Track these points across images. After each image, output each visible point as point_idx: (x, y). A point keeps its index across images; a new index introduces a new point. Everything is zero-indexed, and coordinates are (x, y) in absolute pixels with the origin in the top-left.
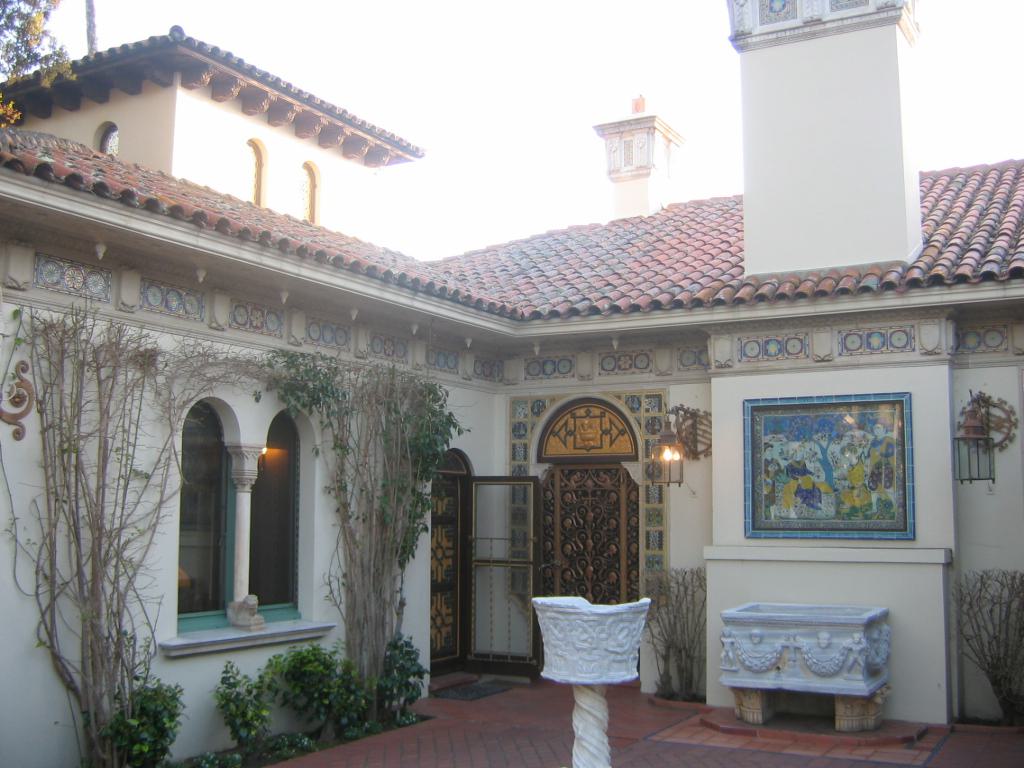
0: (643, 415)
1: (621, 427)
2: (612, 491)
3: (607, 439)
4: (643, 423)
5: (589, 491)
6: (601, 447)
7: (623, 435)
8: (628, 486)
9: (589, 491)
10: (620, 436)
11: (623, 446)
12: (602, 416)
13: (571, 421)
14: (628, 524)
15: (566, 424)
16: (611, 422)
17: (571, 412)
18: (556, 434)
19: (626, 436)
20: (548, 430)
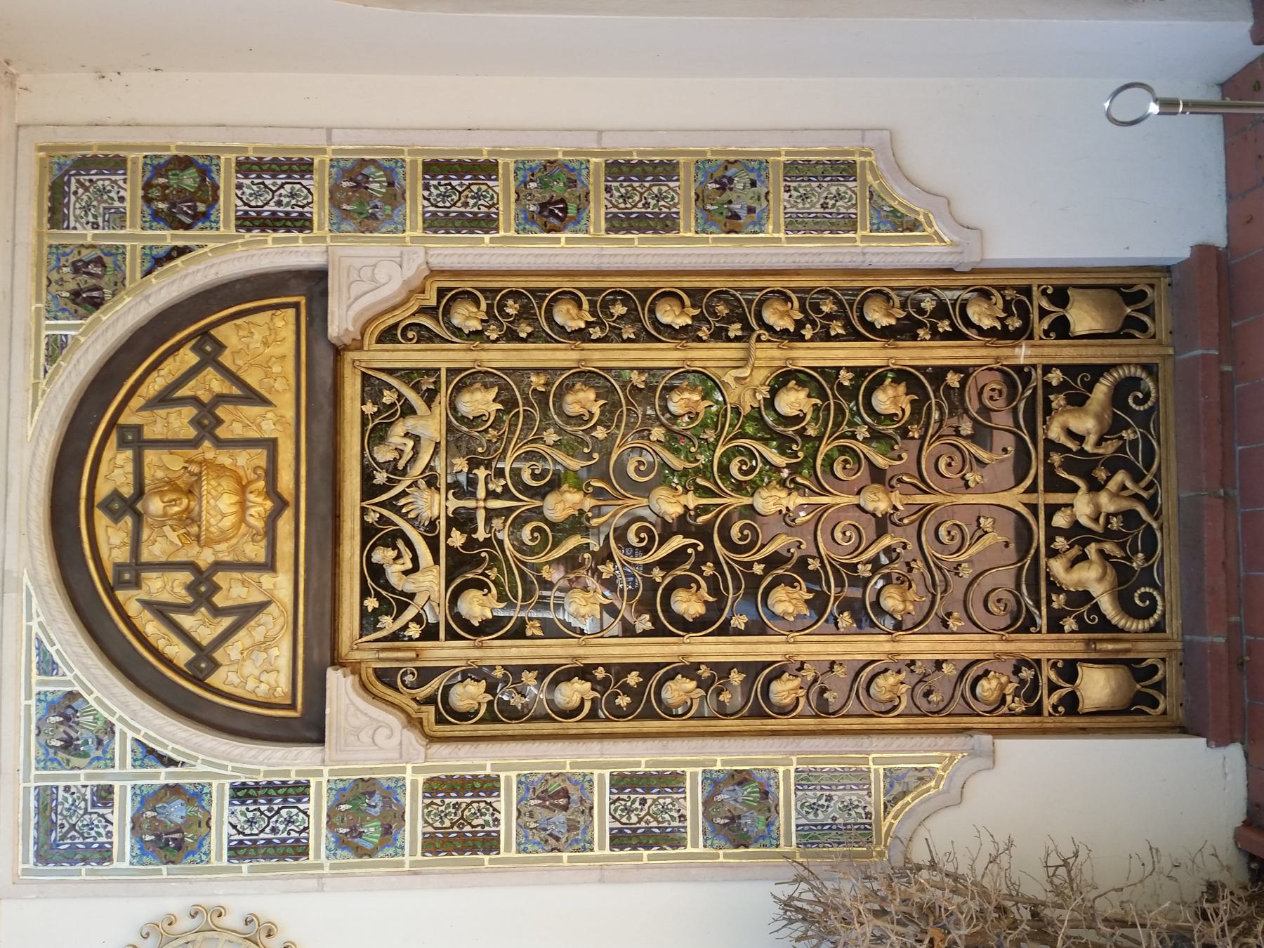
0: (137, 236)
1: (188, 357)
2: (453, 407)
3: (235, 422)
4: (169, 238)
5: (454, 504)
6: (271, 445)
7: (220, 347)
8: (432, 337)
9: (454, 504)
10: (226, 359)
11: (264, 345)
12: (135, 441)
13: (159, 586)
14: (581, 335)
15: (161, 610)
16: (165, 399)
17: (110, 591)
18: (206, 658)
19: (221, 333)
20: (186, 693)
